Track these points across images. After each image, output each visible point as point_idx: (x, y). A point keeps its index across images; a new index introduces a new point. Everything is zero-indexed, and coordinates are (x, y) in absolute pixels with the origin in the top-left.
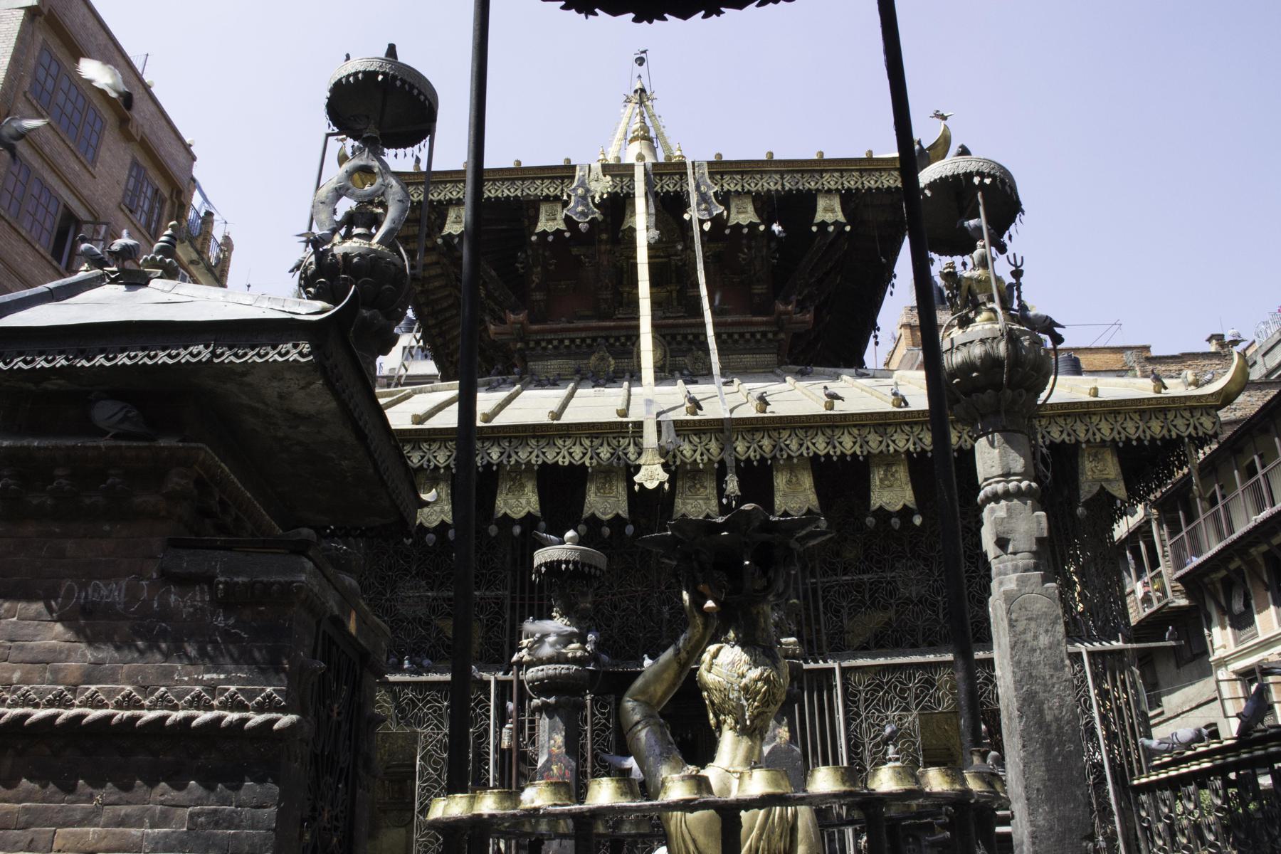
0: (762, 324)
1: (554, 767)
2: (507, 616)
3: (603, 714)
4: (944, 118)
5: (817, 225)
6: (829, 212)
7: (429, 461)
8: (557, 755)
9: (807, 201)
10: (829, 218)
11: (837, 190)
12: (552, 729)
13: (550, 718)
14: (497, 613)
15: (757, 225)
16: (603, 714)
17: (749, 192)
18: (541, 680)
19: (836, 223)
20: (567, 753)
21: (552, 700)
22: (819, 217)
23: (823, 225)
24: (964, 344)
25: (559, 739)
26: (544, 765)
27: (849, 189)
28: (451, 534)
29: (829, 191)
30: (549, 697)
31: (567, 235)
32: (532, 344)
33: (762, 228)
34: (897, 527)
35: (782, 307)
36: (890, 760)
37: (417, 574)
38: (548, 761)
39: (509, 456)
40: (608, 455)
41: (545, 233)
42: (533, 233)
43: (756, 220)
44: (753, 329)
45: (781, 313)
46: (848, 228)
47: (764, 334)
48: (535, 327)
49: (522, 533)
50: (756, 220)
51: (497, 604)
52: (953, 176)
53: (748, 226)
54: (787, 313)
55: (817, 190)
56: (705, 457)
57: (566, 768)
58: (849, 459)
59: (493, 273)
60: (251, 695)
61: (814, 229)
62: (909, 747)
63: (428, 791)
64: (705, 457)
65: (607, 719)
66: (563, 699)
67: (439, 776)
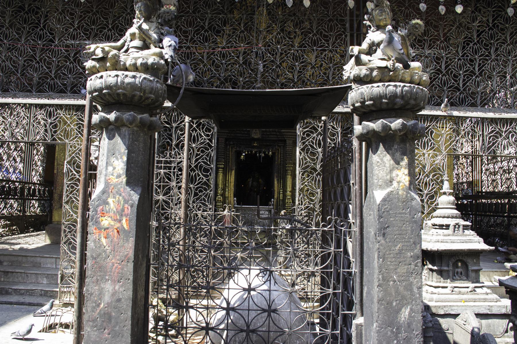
1: (110, 200)
3: (208, 136)
8: (115, 186)
12: (112, 153)
13: (111, 138)
16: (208, 136)
20: (128, 183)
21: (112, 116)
25: (120, 165)
26: (99, 198)
30: (109, 112)
34: (443, 13)
36: (445, 193)
37: (78, 27)
38: (104, 192)
57: (126, 201)
62: (438, 178)
63: (72, 187)
65: (210, 140)
66: (127, 116)
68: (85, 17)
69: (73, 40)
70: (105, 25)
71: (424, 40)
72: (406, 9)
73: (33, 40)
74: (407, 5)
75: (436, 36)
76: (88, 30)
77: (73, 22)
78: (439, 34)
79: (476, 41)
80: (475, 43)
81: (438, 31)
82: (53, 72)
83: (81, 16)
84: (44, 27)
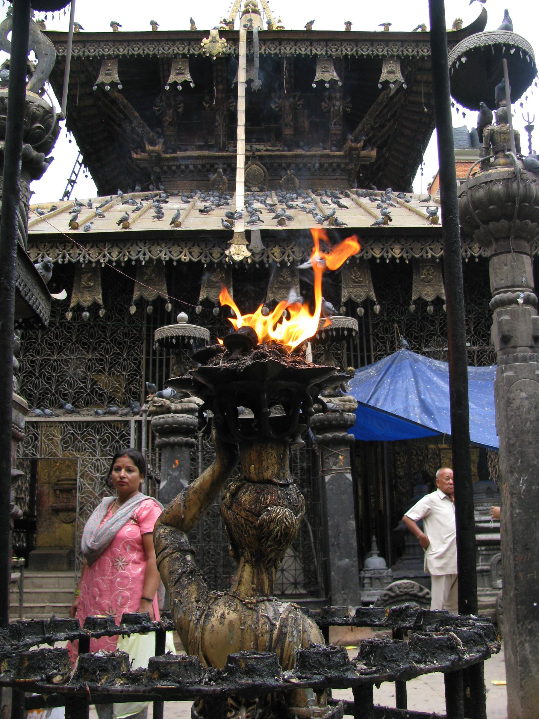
0: (338, 157)
2: (143, 373)
5: (381, 83)
6: (392, 74)
7: (84, 257)
10: (391, 78)
11: (398, 57)
14: (135, 370)
15: (336, 81)
17: (331, 56)
18: (162, 425)
22: (384, 76)
23: (386, 83)
24: (486, 183)
27: (407, 56)
28: (102, 313)
29: (392, 57)
31: (192, 85)
32: (165, 168)
33: (340, 84)
35: (353, 145)
37: (77, 342)
40: (219, 255)
41: (175, 84)
42: (165, 84)
43: (336, 78)
44: (331, 161)
45: (351, 149)
47: (339, 165)
48: (168, 156)
49: (155, 310)
50: (336, 78)
51: (135, 364)
52: (485, 46)
53: (329, 82)
54: (356, 149)
55: (383, 56)
56: (291, 258)
58: (398, 261)
64: (291, 258)
67: (94, 489)
68: (82, 331)
69: (73, 353)
70: (103, 338)
71: (421, 336)
72: (401, 306)
73: (31, 355)
74: (401, 302)
75: (432, 331)
76: (86, 344)
77: (71, 336)
78: (435, 329)
79: (473, 333)
80: (473, 335)
81: (433, 326)
82: (54, 387)
83: (79, 330)
84: (42, 341)
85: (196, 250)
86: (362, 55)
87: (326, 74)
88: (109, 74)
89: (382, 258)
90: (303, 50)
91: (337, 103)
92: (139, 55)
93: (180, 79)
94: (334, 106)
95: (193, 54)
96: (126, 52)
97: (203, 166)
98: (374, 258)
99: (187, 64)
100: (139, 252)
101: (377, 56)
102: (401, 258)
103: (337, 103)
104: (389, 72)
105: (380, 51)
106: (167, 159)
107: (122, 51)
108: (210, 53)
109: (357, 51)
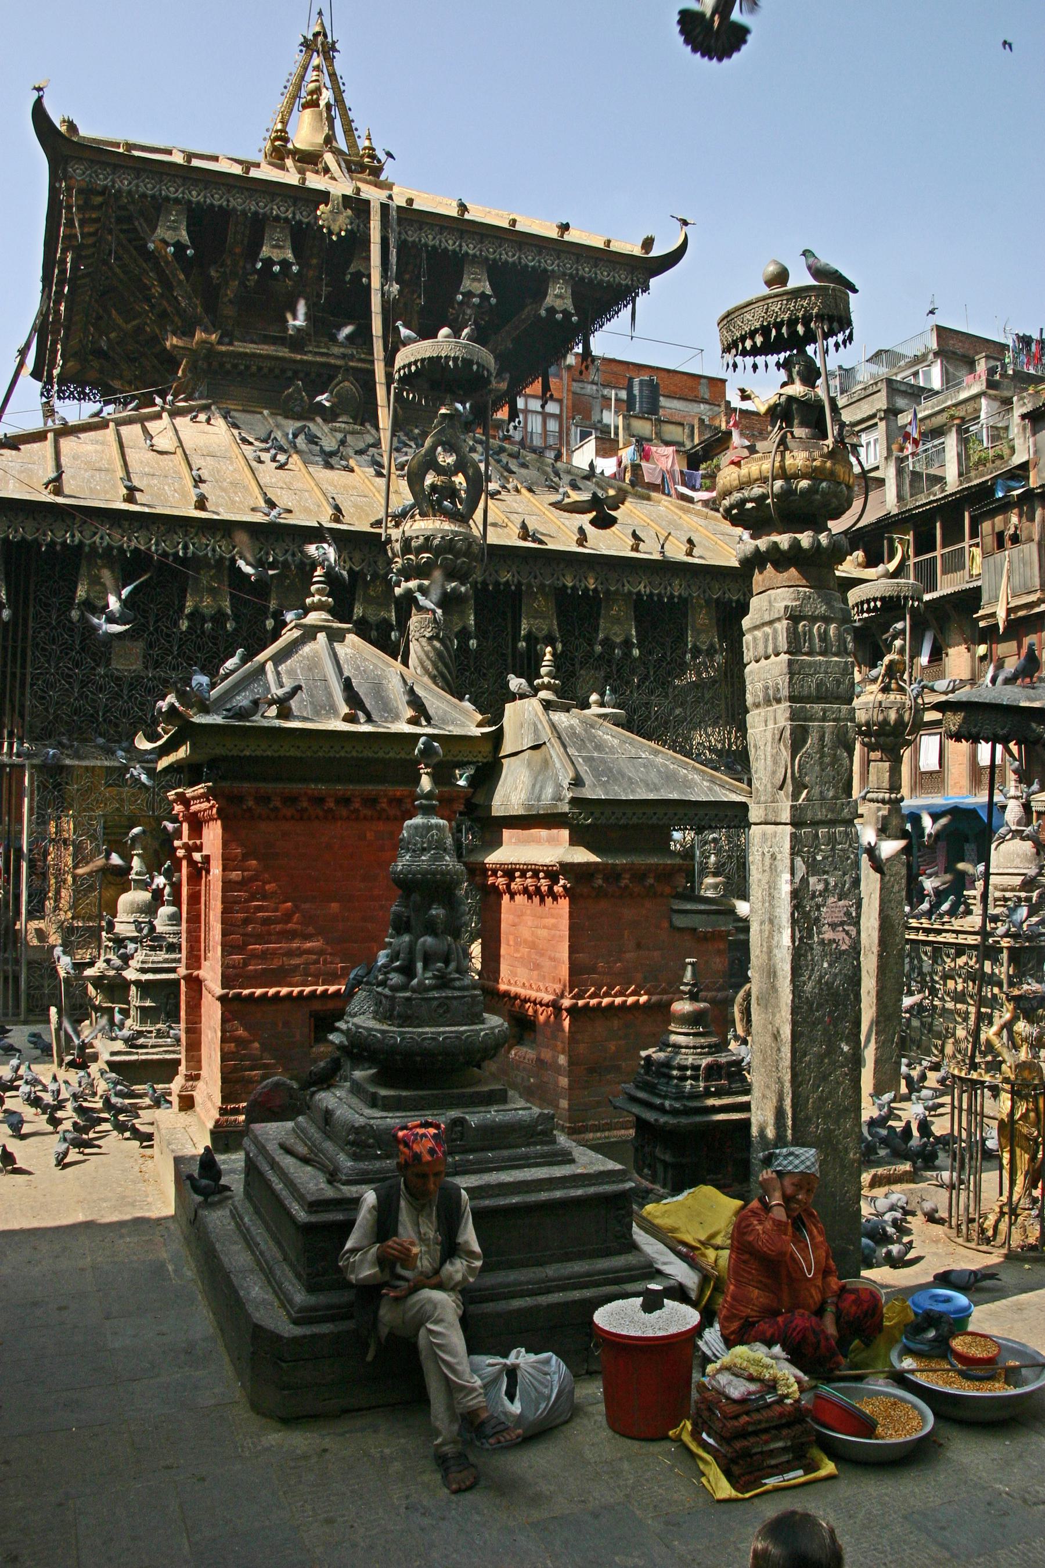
4: (685, 223)
6: (558, 297)
7: (214, 550)
9: (540, 282)
10: (558, 304)
17: (487, 259)
19: (565, 312)
22: (549, 300)
27: (582, 278)
33: (493, 301)
39: (294, 555)
43: (489, 292)
46: (575, 319)
48: (223, 348)
50: (489, 292)
59: (182, 277)
60: (715, 983)
61: (543, 313)
85: (357, 556)
86: (527, 266)
87: (476, 284)
88: (175, 229)
89: (574, 588)
90: (451, 244)
91: (469, 311)
92: (220, 207)
93: (276, 255)
94: (464, 314)
95: (300, 222)
96: (201, 198)
97: (271, 370)
98: (565, 586)
99: (287, 232)
100: (287, 551)
101: (545, 270)
102: (595, 590)
103: (469, 311)
104: (557, 296)
105: (551, 265)
106: (223, 354)
107: (195, 196)
108: (329, 228)
109: (520, 258)
